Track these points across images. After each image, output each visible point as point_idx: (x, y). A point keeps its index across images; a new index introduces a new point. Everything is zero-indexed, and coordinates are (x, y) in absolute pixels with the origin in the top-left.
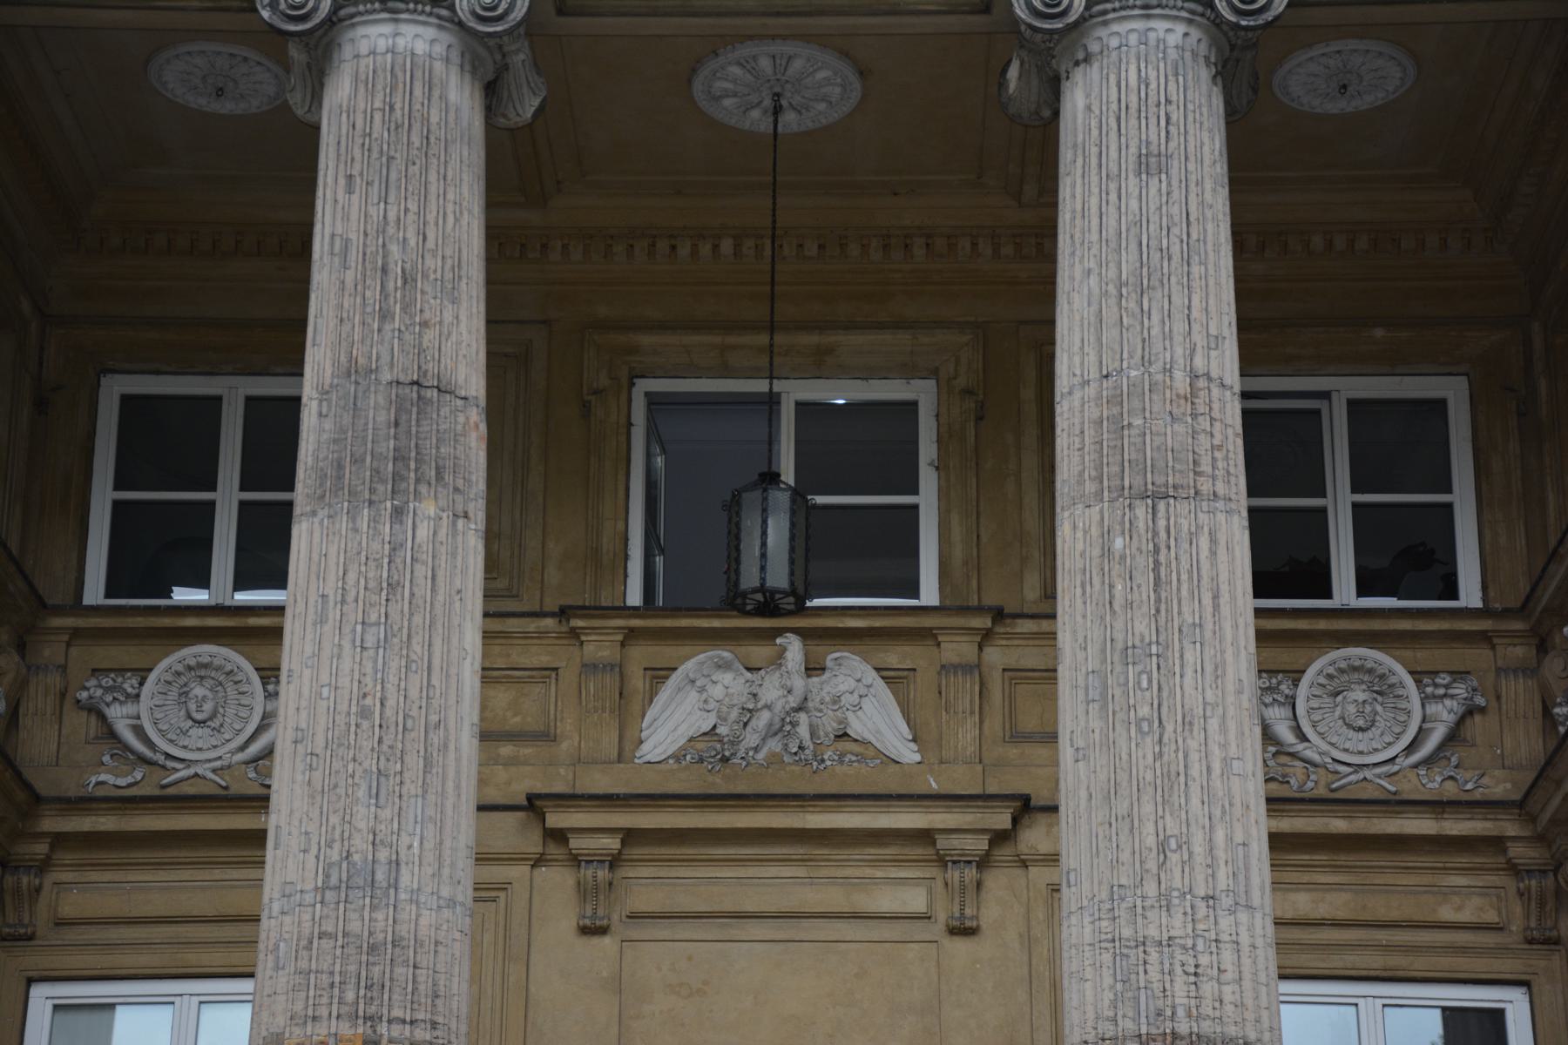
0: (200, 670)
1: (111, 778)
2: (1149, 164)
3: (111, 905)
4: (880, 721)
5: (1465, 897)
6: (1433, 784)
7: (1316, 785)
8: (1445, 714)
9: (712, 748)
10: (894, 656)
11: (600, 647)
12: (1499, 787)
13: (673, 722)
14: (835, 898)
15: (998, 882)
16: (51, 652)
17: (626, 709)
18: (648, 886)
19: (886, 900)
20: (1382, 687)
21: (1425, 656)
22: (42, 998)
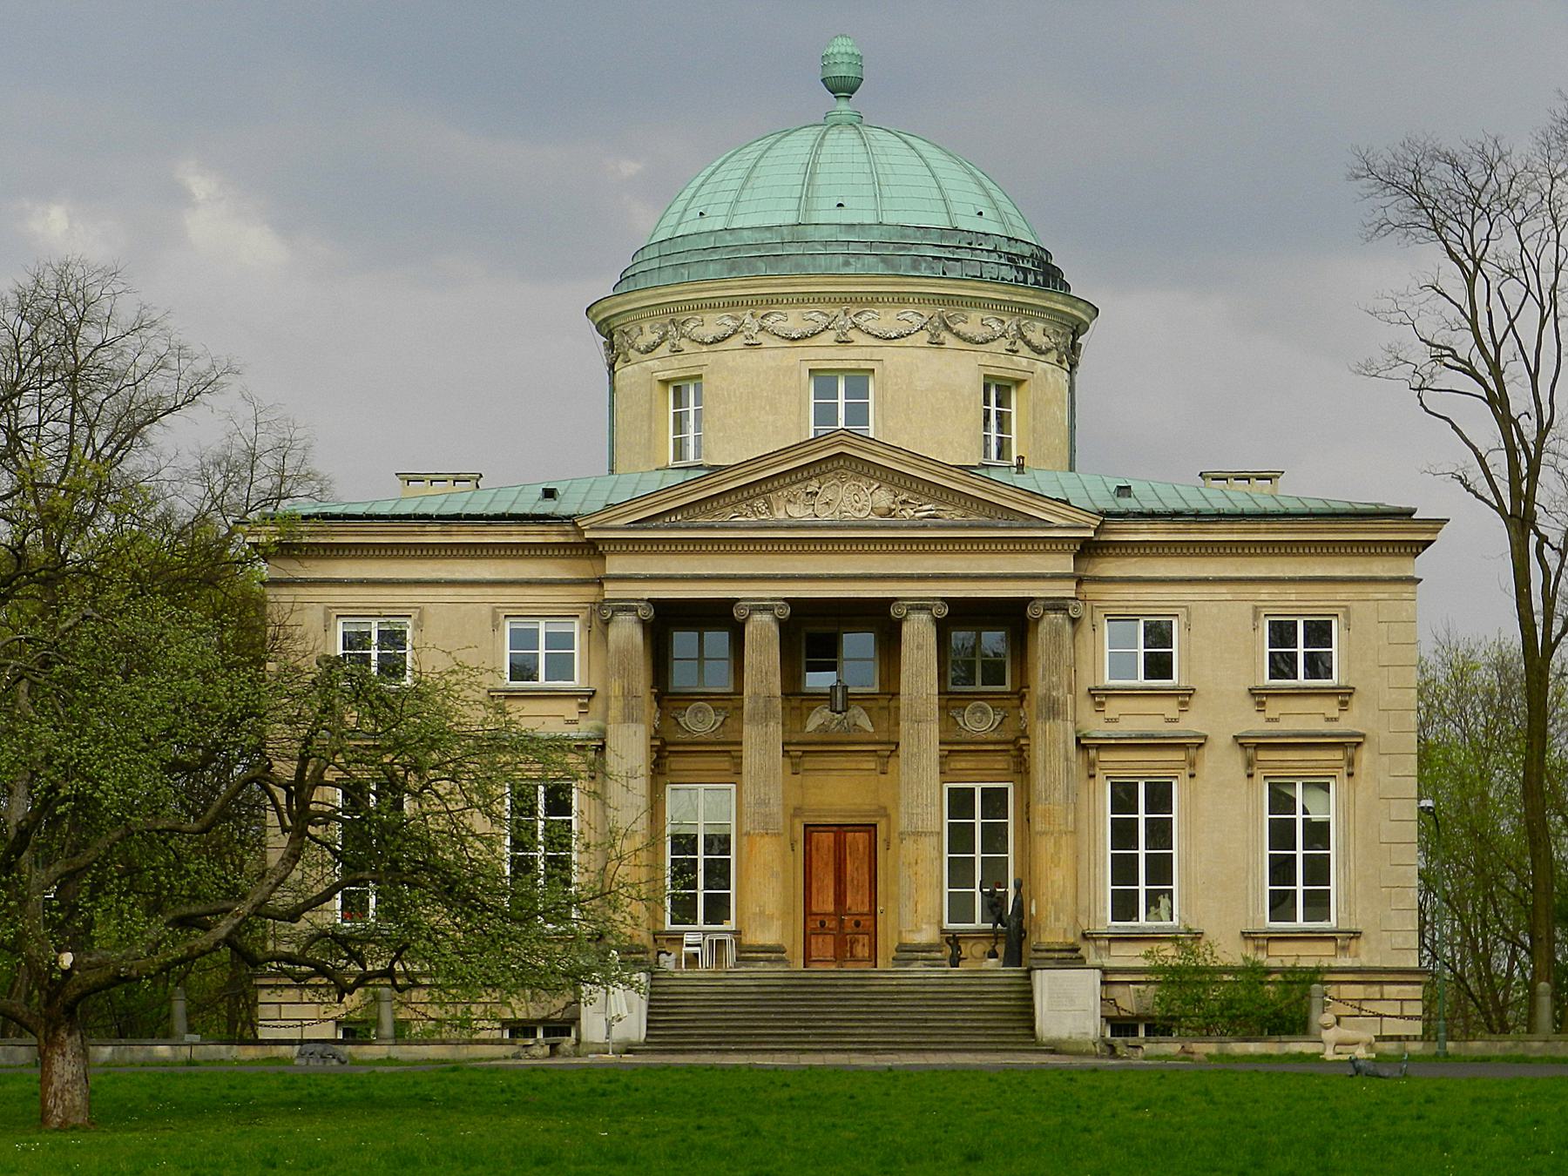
0: (700, 709)
1: (680, 736)
2: (919, 647)
3: (682, 766)
4: (865, 722)
5: (1001, 762)
6: (995, 736)
7: (968, 737)
8: (999, 718)
9: (822, 728)
10: (867, 704)
11: (795, 702)
12: (1011, 737)
13: (813, 722)
14: (854, 766)
15: (891, 760)
16: (665, 704)
17: (803, 719)
18: (809, 763)
19: (865, 766)
20: (984, 712)
21: (996, 703)
22: (669, 787)
